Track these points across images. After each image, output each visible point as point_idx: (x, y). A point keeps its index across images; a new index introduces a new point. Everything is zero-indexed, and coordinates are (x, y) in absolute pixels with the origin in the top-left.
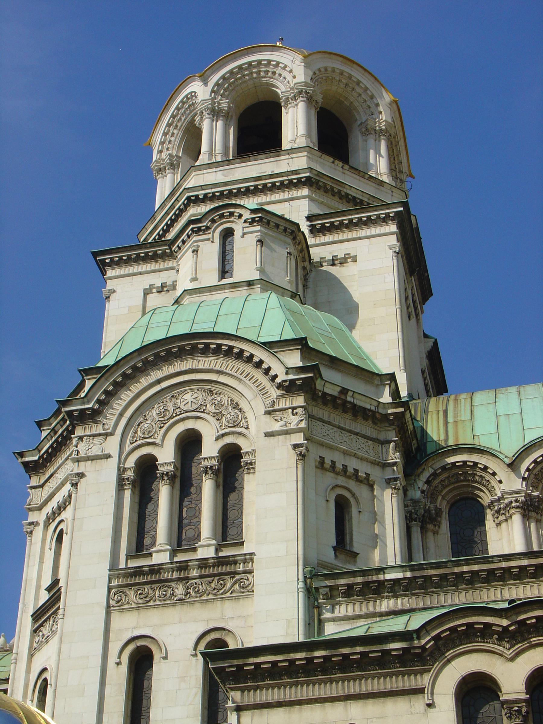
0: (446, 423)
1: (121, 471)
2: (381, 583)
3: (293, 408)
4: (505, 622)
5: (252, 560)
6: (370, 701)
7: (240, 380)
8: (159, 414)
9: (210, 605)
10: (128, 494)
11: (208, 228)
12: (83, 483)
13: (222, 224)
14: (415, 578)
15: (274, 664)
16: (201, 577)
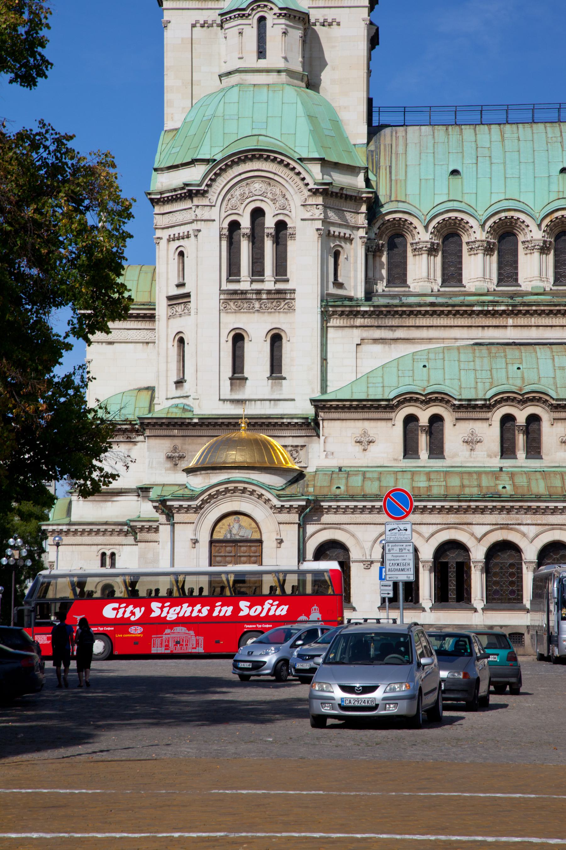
0: (391, 180)
1: (221, 229)
2: (358, 312)
3: (317, 205)
4: (424, 398)
5: (294, 293)
6: (372, 421)
7: (287, 181)
8: (241, 195)
9: (272, 315)
10: (224, 243)
11: (249, 15)
12: (200, 235)
13: (258, 12)
14: (375, 311)
15: (338, 405)
16: (267, 299)
